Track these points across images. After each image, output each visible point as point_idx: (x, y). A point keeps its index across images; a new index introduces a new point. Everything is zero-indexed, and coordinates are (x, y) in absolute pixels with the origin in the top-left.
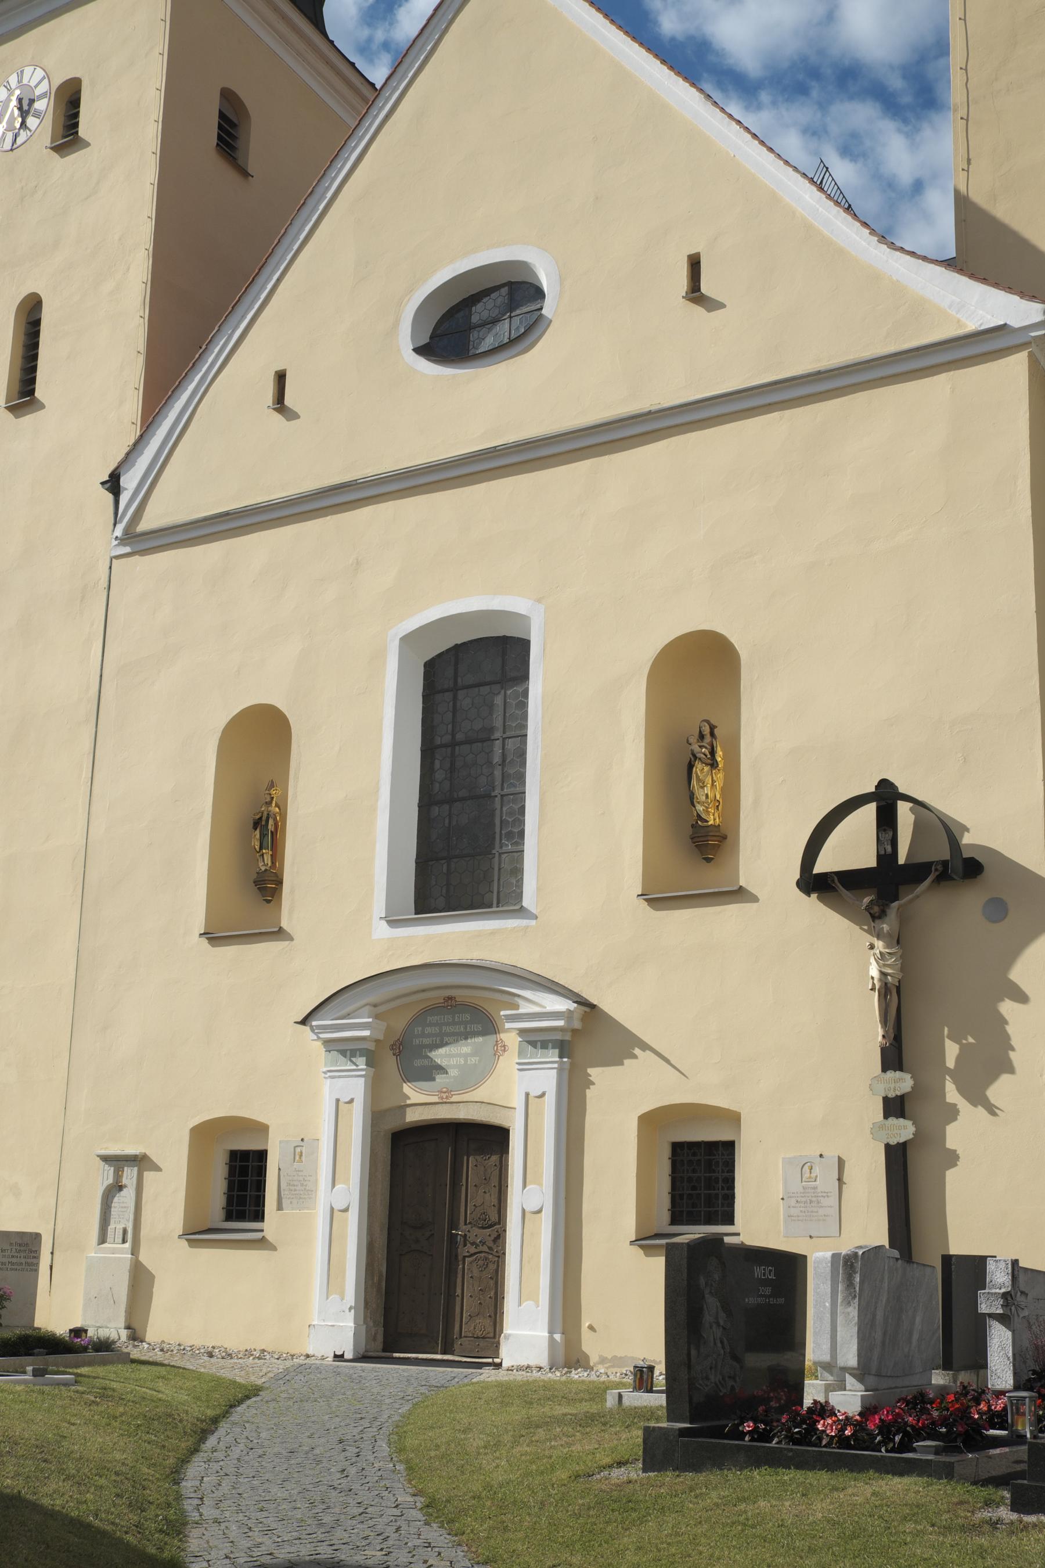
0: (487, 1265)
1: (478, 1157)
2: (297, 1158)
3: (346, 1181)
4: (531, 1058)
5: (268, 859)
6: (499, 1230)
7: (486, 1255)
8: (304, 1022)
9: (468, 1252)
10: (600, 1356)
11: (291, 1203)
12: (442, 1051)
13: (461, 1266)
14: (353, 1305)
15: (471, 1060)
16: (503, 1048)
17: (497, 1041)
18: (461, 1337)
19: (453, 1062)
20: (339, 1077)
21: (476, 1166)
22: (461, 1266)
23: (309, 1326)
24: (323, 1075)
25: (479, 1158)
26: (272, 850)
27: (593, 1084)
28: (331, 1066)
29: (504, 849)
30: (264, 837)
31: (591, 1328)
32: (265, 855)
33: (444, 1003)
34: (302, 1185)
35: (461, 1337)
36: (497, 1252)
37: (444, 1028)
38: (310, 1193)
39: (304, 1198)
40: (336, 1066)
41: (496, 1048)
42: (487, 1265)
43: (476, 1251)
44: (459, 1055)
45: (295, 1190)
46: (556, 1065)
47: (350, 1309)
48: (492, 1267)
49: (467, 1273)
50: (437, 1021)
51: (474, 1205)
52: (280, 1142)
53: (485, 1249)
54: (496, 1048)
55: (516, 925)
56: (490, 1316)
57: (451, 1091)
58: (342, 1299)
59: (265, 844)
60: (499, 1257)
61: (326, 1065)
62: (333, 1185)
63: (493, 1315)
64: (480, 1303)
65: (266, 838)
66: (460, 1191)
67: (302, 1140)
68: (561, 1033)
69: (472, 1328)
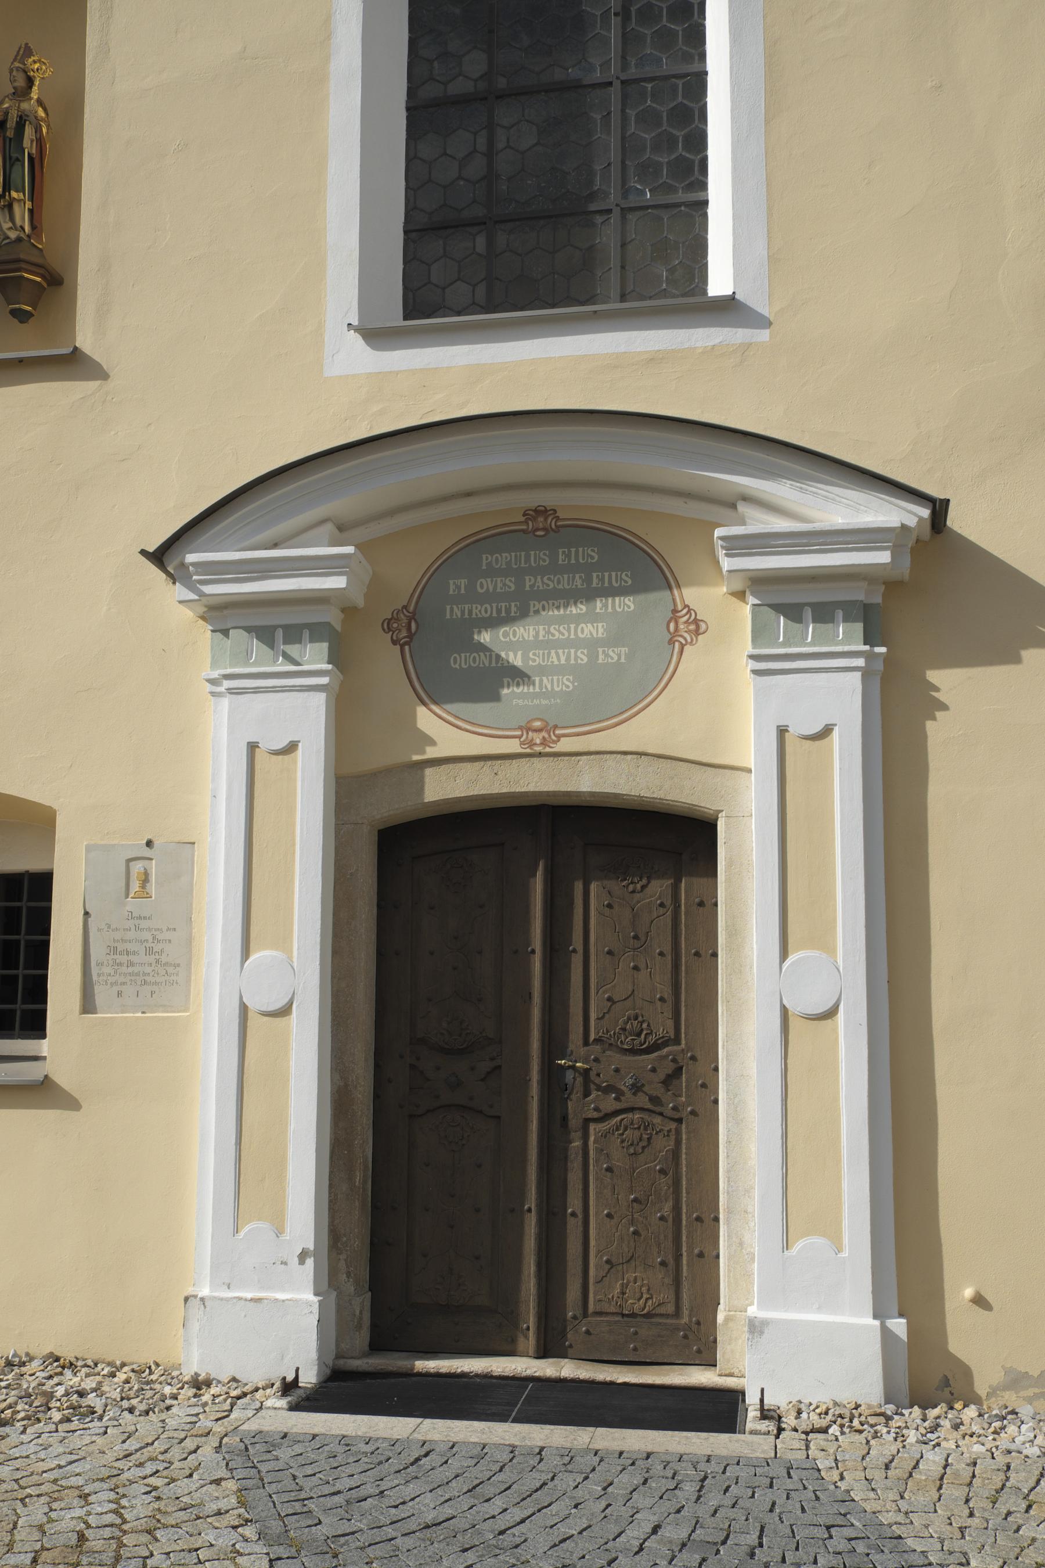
0: (649, 1139)
1: (607, 883)
2: (135, 886)
3: (283, 942)
4: (786, 643)
5: (22, 214)
6: (679, 1059)
7: (645, 1116)
8: (159, 557)
9: (596, 1109)
10: (1008, 1371)
11: (119, 994)
12: (524, 631)
13: (577, 1144)
14: (311, 1247)
15: (607, 655)
16: (692, 627)
17: (675, 611)
18: (585, 1315)
19: (558, 658)
20: (256, 690)
21: (610, 906)
22: (577, 1144)
23: (186, 1299)
24: (209, 687)
25: (616, 886)
26: (32, 199)
27: (944, 707)
28: (231, 666)
29: (633, 201)
30: (12, 166)
31: (979, 1301)
32: (17, 208)
33: (526, 522)
34: (149, 951)
35: (585, 1315)
36: (675, 1108)
37: (529, 581)
38: (170, 970)
39: (156, 983)
40: (246, 663)
41: (672, 626)
42: (649, 1139)
43: (618, 1106)
44: (575, 644)
45: (131, 964)
46: (860, 662)
47: (303, 1257)
48: (663, 1145)
49: (597, 1161)
50: (509, 563)
51: (609, 999)
52: (89, 849)
53: (642, 1101)
54: (672, 626)
55: (717, 341)
56: (663, 1264)
57: (556, 727)
58: (279, 1232)
59: (15, 176)
60: (680, 1121)
61: (214, 665)
62: (784, 954)
63: (671, 1262)
64: (636, 1233)
65: (17, 167)
66: (568, 966)
67: (149, 844)
68: (864, 584)
69: (617, 1291)
